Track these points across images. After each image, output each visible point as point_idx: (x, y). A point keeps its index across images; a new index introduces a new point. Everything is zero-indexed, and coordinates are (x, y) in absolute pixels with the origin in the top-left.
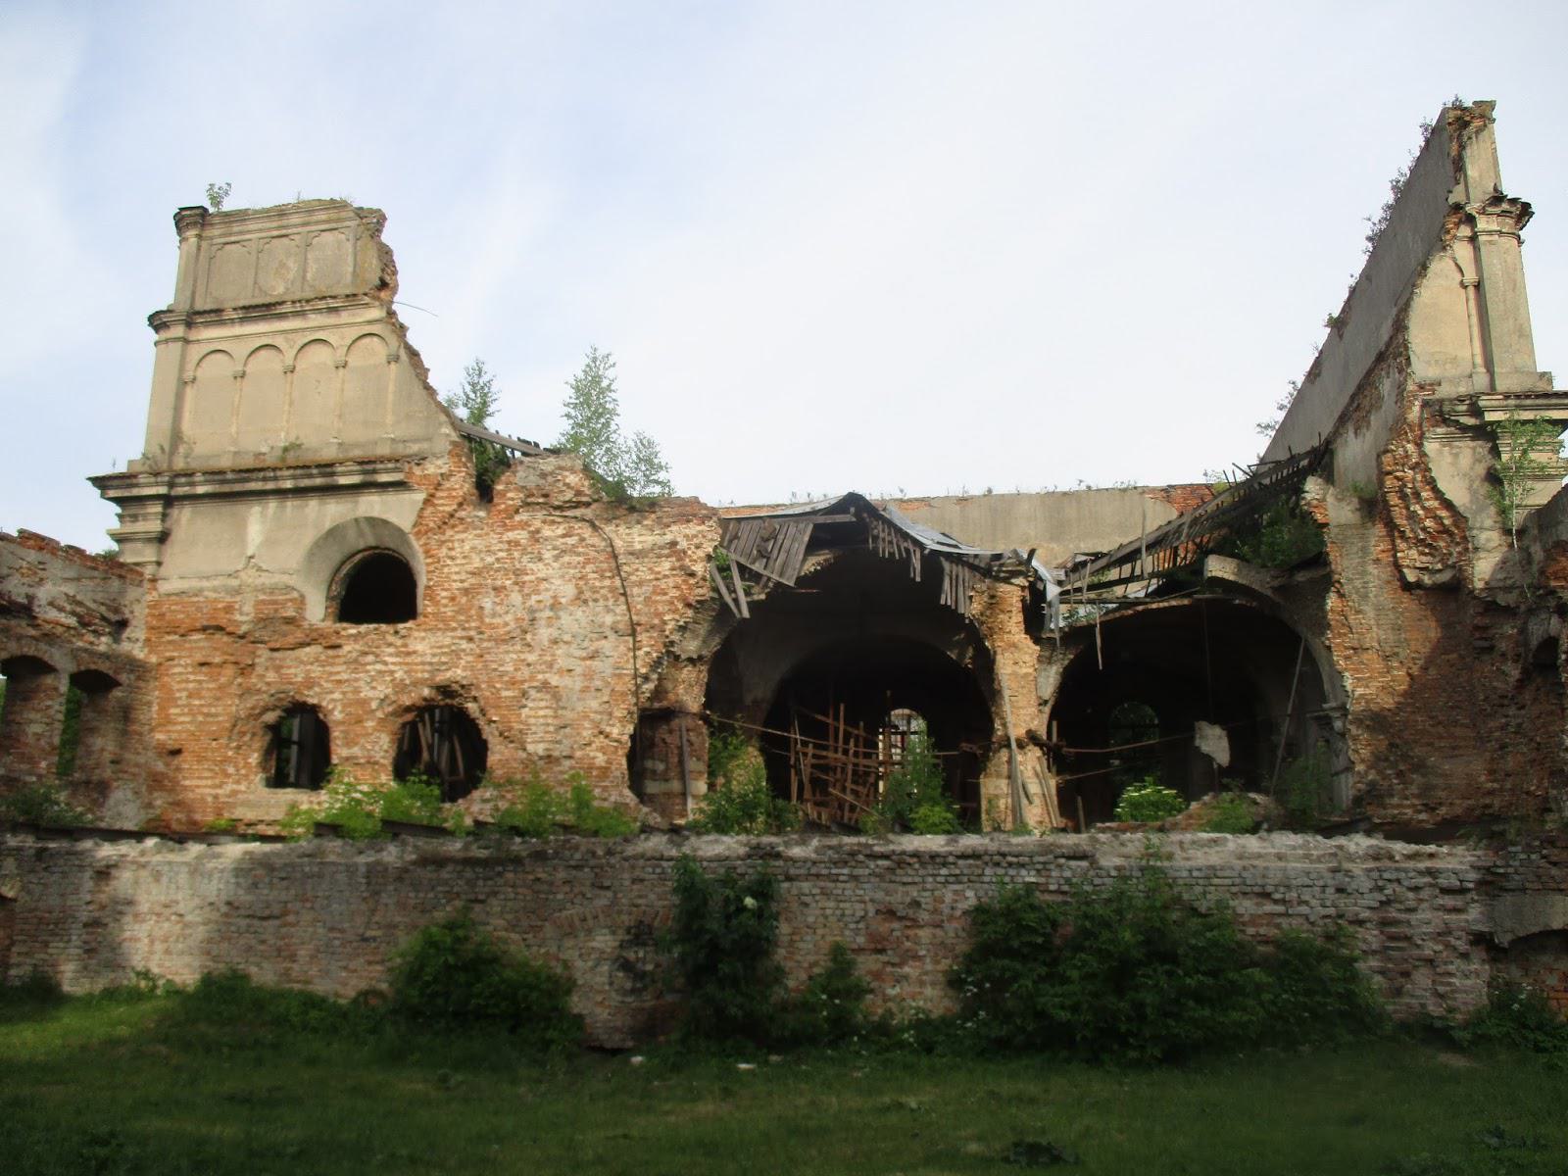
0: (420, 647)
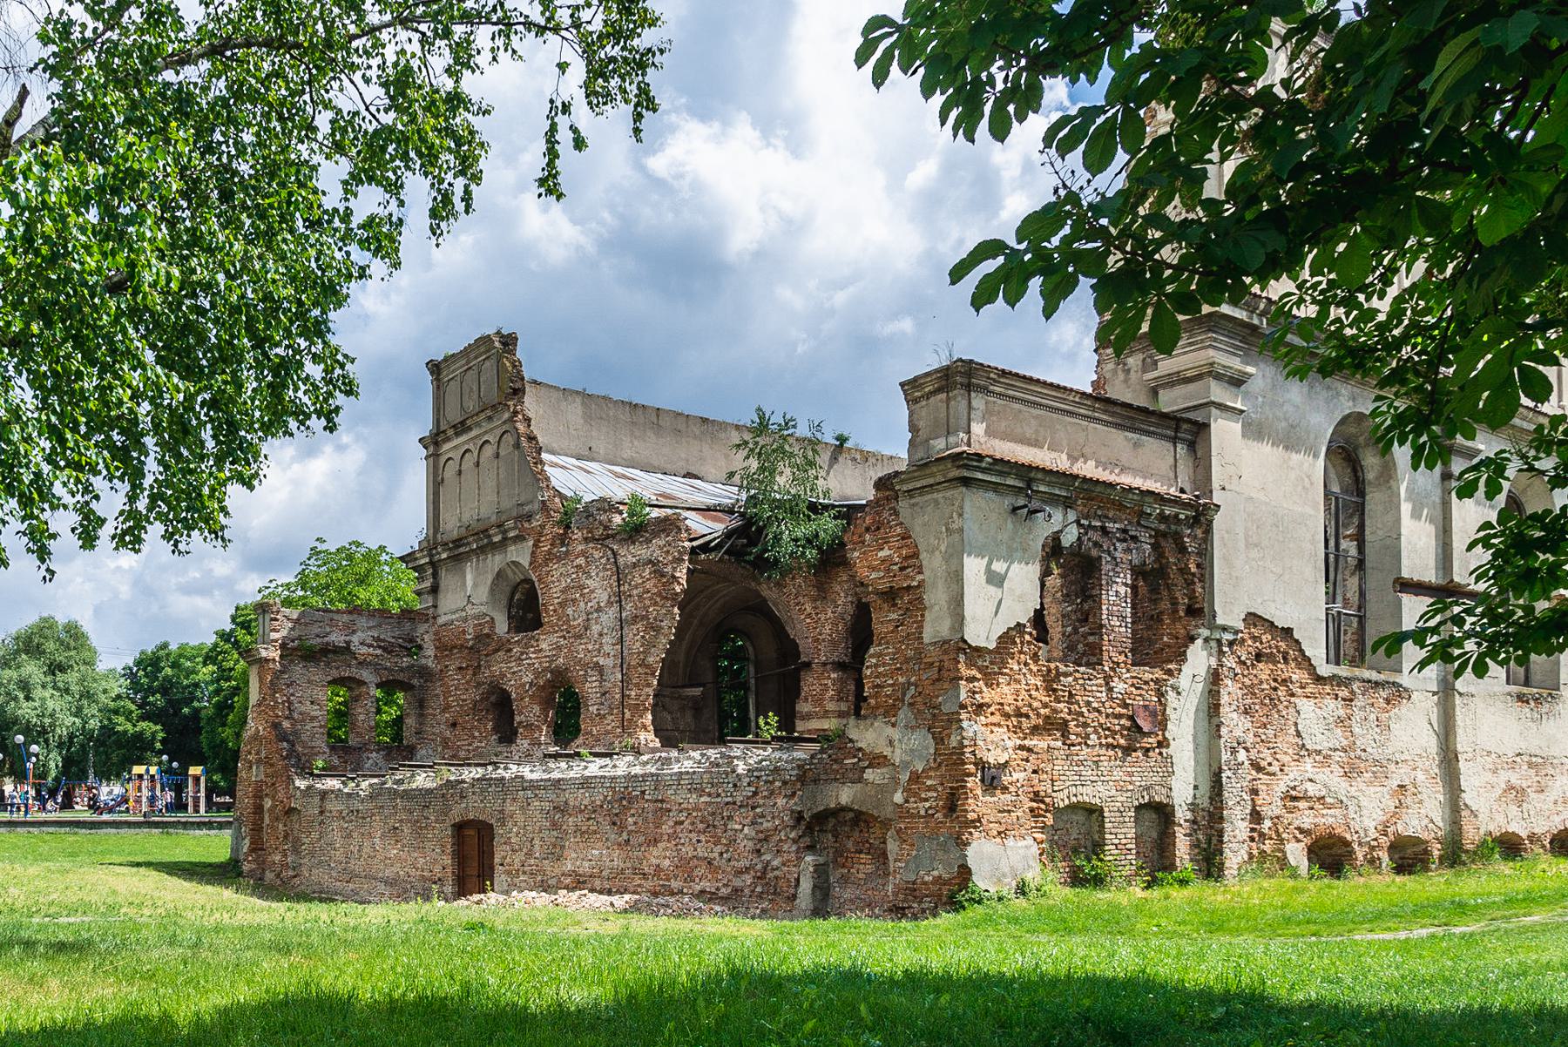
0: (544, 646)
